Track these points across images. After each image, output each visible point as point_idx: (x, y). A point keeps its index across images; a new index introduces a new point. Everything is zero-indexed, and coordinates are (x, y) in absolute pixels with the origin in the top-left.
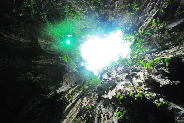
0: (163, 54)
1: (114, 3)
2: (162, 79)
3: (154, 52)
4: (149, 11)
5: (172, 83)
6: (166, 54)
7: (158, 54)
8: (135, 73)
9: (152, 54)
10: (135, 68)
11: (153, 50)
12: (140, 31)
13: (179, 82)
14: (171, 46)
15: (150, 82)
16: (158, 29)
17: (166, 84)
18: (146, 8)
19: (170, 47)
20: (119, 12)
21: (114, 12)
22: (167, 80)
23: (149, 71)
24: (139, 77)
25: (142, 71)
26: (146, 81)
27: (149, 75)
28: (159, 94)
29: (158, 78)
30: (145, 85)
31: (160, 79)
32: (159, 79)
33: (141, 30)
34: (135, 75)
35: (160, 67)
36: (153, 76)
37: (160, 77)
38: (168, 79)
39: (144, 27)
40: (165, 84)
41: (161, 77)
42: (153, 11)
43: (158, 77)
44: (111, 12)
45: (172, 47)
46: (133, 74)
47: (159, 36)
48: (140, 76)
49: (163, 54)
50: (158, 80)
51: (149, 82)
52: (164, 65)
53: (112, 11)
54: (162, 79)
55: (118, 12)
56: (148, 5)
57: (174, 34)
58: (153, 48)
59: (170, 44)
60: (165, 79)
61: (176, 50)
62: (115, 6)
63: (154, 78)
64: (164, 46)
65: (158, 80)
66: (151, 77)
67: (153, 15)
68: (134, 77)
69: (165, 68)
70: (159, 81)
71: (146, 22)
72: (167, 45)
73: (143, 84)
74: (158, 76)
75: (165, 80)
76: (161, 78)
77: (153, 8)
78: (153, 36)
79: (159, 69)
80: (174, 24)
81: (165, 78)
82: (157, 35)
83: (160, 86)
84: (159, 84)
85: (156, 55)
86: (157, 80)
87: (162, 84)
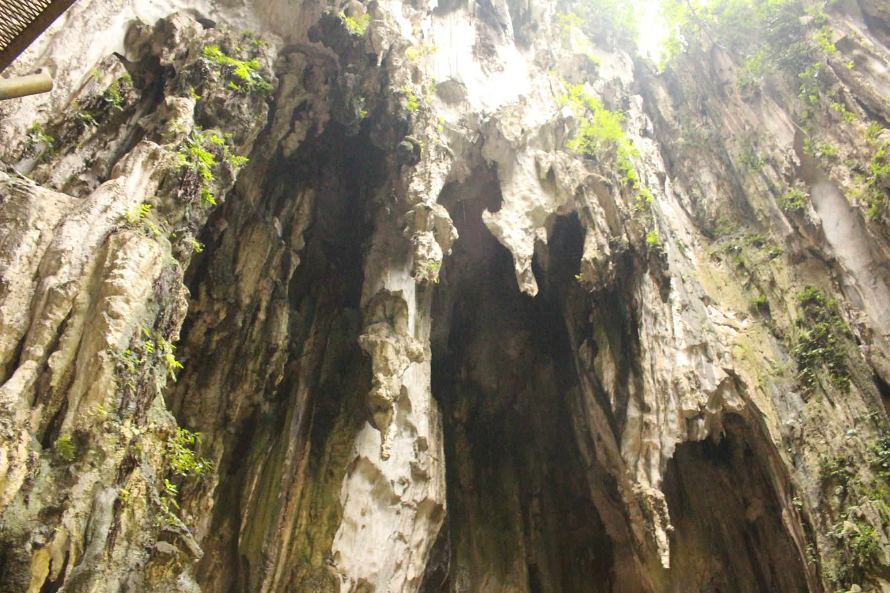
0: (651, 172)
2: (527, 214)
3: (649, 109)
5: (526, 270)
6: (654, 185)
7: (645, 133)
8: (504, 27)
9: (639, 99)
10: (535, 15)
11: (661, 93)
12: (837, 36)
13: (535, 293)
14: (694, 201)
15: (490, 153)
16: (834, 159)
17: (508, 241)
19: (688, 190)
22: (527, 238)
23: (558, 131)
24: (492, 66)
25: (537, 81)
26: (485, 130)
27: (529, 138)
28: (455, 231)
29: (527, 193)
30: (462, 123)
31: (525, 204)
32: (525, 198)
33: (846, 45)
34: (495, 27)
35: (601, 204)
36: (527, 164)
37: (537, 204)
38: (538, 242)
39: (860, 63)
40: (510, 236)
41: (539, 209)
43: (531, 191)
45: (686, 200)
46: (494, 11)
47: (772, 150)
48: (501, 69)
49: (651, 172)
50: (513, 194)
51: (487, 148)
52: (616, 223)
54: (527, 214)
57: (779, 228)
58: (673, 90)
59: (704, 195)
60: (531, 227)
61: (679, 238)
63: (522, 169)
64: (694, 161)
65: (513, 194)
66: (522, 148)
68: (479, 28)
69: (603, 232)
70: (509, 203)
72: (699, 176)
73: (461, 108)
74: (539, 191)
75: (526, 230)
76: (529, 207)
78: (783, 115)
79: (592, 201)
80: (838, 224)
81: (536, 226)
82: (785, 141)
83: (486, 215)
84: (495, 204)
85: (639, 125)
86: (516, 191)
87: (500, 223)
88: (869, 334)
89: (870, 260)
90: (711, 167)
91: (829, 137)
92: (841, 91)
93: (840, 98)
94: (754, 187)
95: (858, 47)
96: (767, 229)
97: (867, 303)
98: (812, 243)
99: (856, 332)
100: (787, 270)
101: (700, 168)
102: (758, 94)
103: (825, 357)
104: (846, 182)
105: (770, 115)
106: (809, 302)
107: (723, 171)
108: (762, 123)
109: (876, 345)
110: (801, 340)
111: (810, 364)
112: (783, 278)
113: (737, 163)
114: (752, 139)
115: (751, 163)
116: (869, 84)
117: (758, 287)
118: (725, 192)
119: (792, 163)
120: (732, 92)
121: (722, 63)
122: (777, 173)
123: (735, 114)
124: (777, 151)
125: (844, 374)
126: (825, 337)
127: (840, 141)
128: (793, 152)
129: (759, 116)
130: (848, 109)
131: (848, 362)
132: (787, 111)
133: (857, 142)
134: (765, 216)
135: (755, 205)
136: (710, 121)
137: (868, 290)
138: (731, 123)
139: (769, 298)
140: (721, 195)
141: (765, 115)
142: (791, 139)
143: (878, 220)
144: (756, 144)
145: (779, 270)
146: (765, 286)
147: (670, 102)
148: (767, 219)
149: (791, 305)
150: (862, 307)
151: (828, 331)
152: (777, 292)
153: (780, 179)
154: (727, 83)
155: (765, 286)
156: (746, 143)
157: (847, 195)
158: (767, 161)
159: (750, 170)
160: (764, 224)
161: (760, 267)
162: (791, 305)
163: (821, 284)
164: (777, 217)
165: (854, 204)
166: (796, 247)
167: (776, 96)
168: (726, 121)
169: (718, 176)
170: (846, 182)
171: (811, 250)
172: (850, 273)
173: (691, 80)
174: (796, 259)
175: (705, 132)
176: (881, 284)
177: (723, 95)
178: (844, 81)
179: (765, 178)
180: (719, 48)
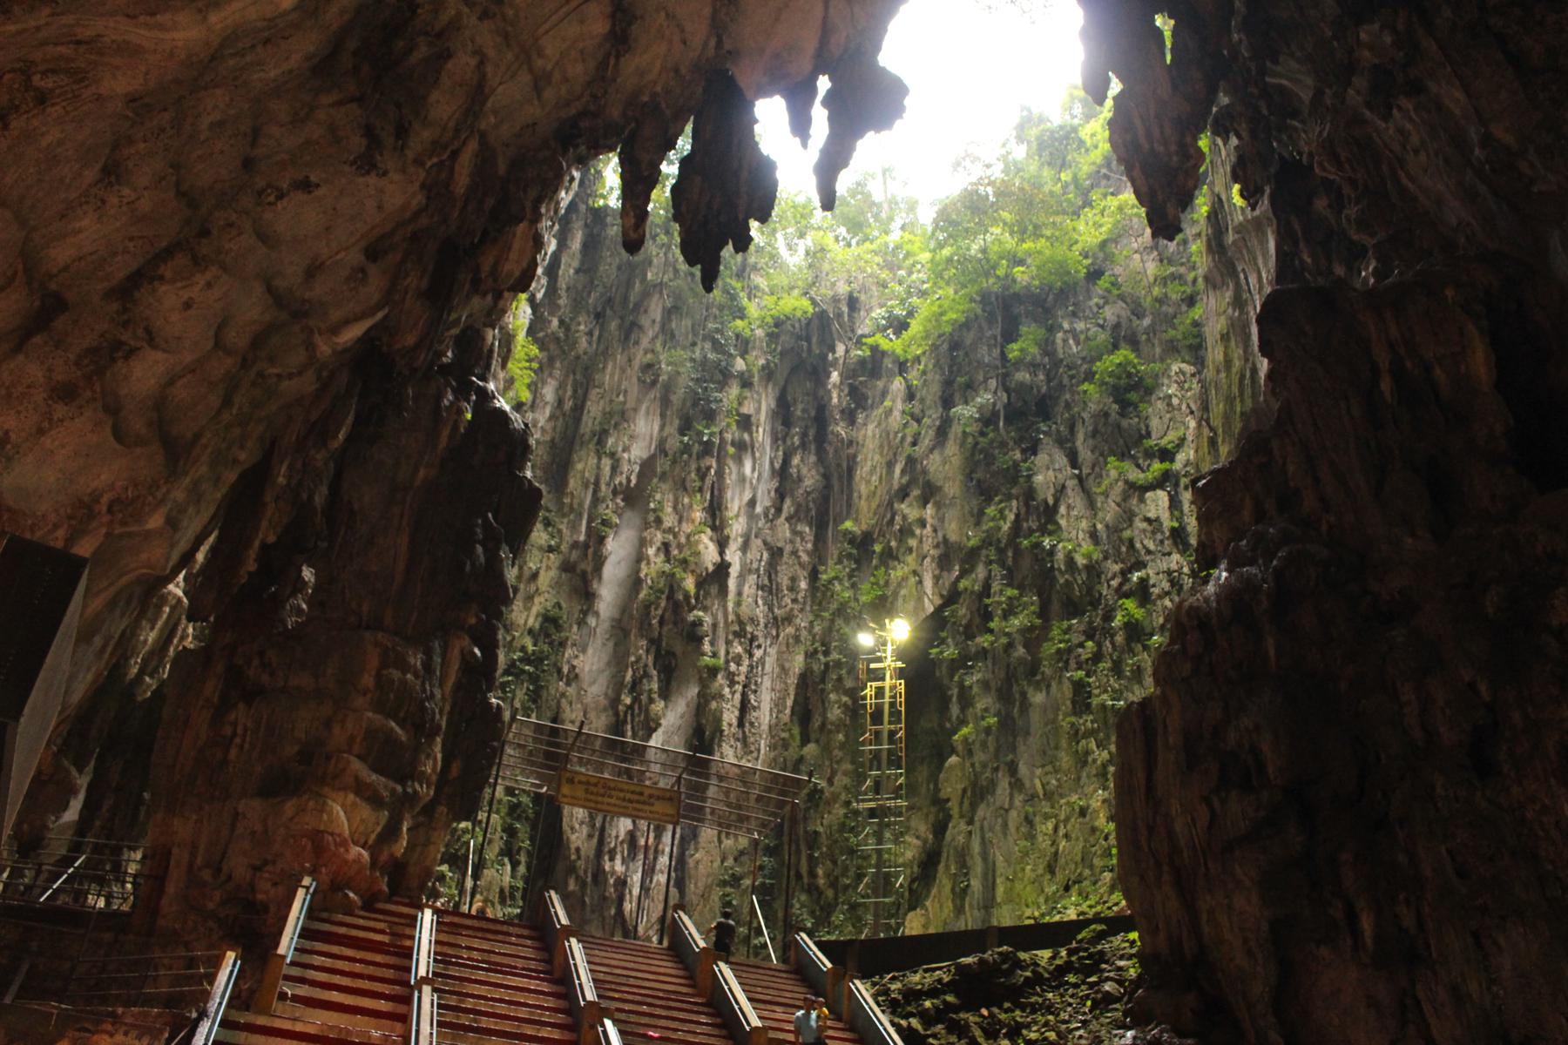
1: (942, 596)
4: (776, 553)
18: (805, 558)
20: (913, 534)
21: (935, 531)
39: (741, 447)
42: (752, 578)
44: (953, 530)
53: (945, 540)
55: (918, 532)
56: (803, 585)
57: (574, 527)
62: (937, 579)
67: (734, 571)
71: (747, 496)
77: (770, 589)
78: (656, 428)
88: (573, 677)
89: (617, 616)
90: (561, 386)
91: (671, 497)
92: (709, 468)
93: (702, 474)
94: (584, 464)
95: (751, 434)
96: (564, 516)
97: (590, 651)
98: (589, 569)
99: (565, 669)
100: (553, 573)
101: (551, 375)
102: (654, 383)
103: (534, 679)
104: (651, 551)
105: (648, 413)
106: (551, 621)
107: (568, 405)
108: (635, 410)
109: (571, 690)
110: (523, 649)
111: (517, 676)
112: (544, 580)
113: (588, 424)
114: (618, 418)
115: (601, 437)
116: (730, 479)
117: (521, 568)
118: (554, 429)
119: (629, 481)
120: (637, 343)
121: (653, 306)
122: (611, 477)
123: (623, 371)
124: (626, 455)
125: (535, 701)
126: (541, 660)
127: (675, 508)
128: (637, 468)
129: (639, 401)
130: (701, 490)
131: (544, 694)
132: (662, 428)
133: (684, 525)
134: (571, 504)
135: (572, 483)
136: (596, 333)
137: (599, 641)
138: (612, 375)
139: (522, 586)
140: (549, 427)
141: (644, 407)
142: (645, 456)
143: (647, 606)
144: (616, 426)
145: (548, 568)
146: (527, 573)
147: (576, 264)
148: (572, 509)
149: (534, 610)
150: (584, 651)
151: (547, 658)
152: (533, 588)
153: (608, 484)
154: (640, 328)
155: (527, 573)
156: (607, 415)
157: (643, 565)
158: (612, 455)
159: (591, 446)
160: (566, 510)
161: (535, 552)
162: (534, 610)
163: (570, 608)
164: (581, 515)
165: (642, 575)
166: (575, 555)
167: (665, 402)
168: (609, 370)
169: (560, 402)
170: (651, 551)
171: (584, 573)
172: (597, 614)
173: (614, 267)
174: (567, 567)
175: (583, 343)
176: (611, 644)
177: (627, 338)
178: (718, 461)
179: (598, 468)
180: (661, 293)
